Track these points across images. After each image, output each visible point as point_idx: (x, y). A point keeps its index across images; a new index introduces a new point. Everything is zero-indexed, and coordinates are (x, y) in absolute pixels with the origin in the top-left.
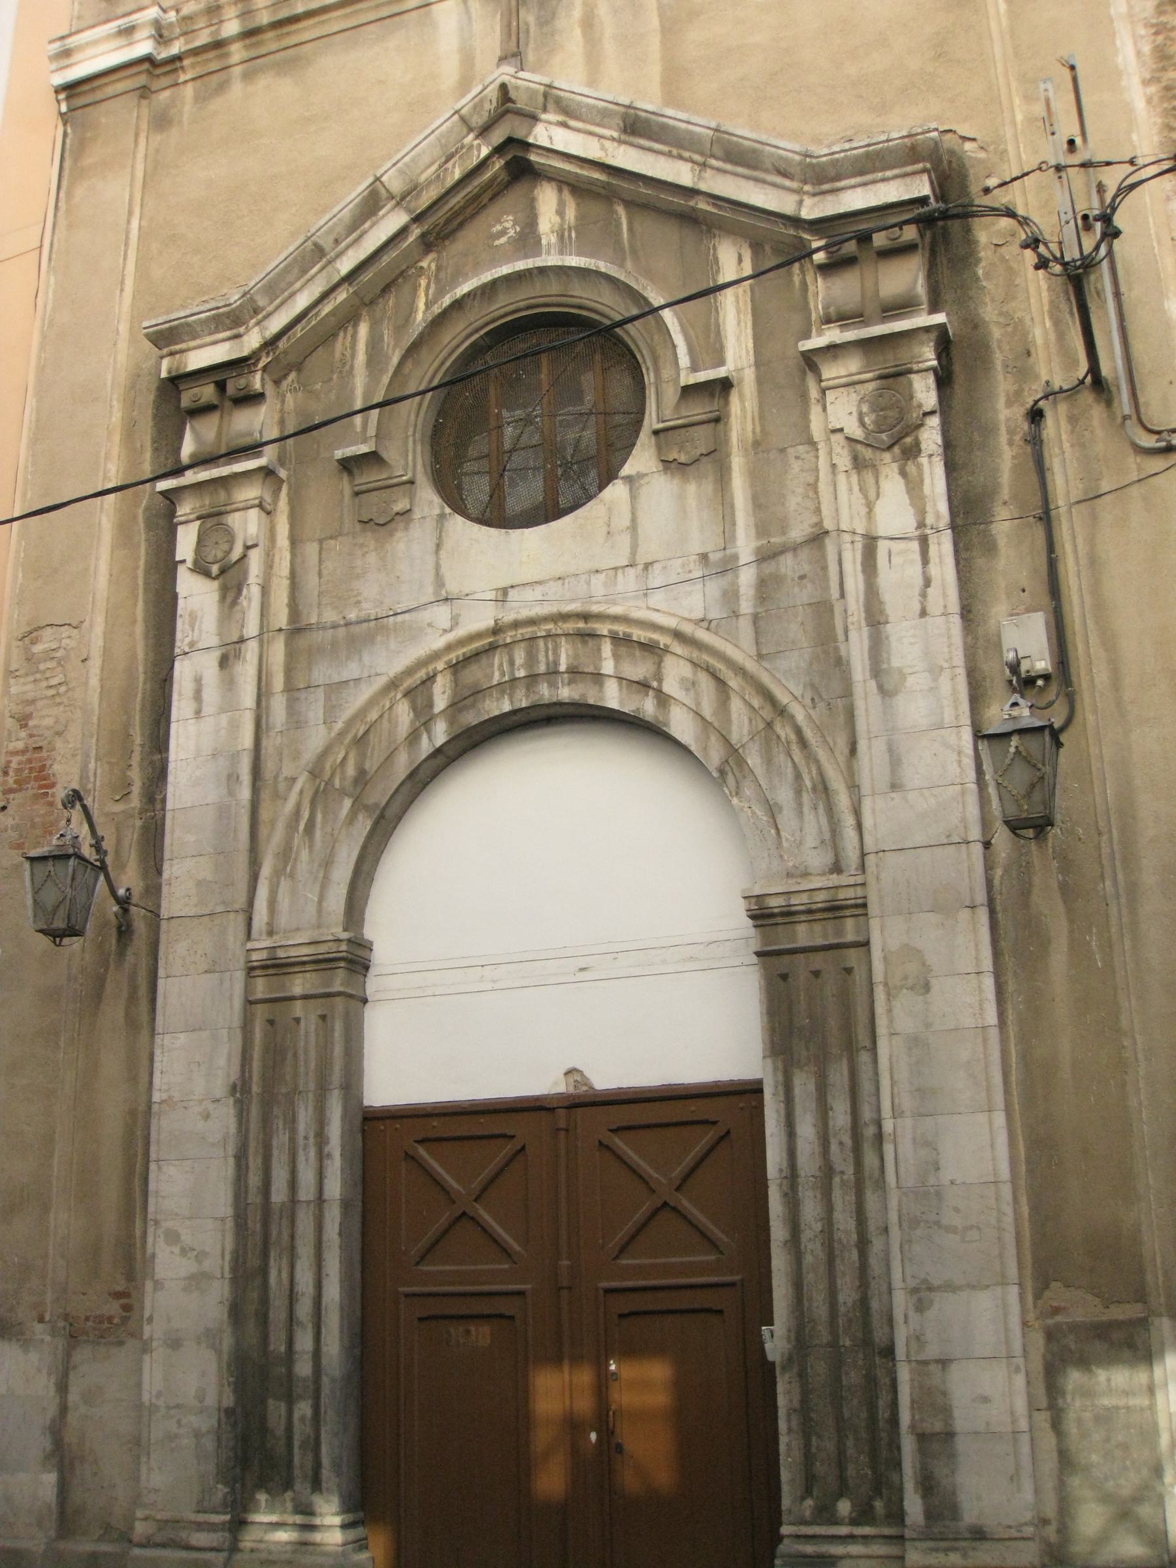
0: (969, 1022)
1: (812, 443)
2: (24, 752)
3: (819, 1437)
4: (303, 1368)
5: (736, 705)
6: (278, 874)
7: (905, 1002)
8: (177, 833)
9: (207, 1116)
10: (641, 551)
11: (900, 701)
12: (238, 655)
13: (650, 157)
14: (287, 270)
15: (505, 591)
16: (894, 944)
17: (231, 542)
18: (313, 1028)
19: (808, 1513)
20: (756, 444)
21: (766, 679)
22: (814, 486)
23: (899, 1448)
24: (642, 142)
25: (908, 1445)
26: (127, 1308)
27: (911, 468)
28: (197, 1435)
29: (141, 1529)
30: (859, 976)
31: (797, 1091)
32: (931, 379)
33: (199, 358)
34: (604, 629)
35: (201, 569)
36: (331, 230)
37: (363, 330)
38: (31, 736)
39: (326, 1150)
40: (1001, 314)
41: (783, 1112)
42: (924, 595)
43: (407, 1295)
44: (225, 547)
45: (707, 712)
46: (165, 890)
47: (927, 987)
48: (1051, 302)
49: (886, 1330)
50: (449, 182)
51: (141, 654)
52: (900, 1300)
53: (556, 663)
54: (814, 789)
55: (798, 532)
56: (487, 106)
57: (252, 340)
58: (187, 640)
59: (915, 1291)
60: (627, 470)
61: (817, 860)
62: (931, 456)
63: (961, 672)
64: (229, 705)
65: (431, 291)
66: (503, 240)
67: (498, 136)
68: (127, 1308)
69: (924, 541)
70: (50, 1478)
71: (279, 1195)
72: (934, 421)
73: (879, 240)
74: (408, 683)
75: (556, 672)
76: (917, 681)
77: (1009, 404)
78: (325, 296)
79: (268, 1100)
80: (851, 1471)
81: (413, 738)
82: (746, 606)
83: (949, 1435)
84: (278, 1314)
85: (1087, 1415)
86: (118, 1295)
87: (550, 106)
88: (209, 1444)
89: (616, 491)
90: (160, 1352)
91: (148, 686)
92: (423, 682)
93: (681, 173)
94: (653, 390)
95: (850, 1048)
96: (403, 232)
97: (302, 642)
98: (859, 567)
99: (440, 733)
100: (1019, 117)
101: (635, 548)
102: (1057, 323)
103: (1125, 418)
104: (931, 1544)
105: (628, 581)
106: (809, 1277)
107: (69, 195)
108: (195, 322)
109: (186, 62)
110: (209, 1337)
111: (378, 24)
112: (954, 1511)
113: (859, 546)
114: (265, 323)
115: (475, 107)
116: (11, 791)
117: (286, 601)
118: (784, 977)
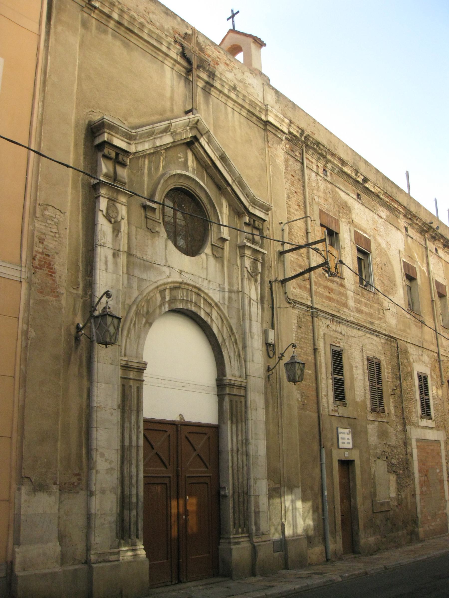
1: (238, 267)
4: (134, 500)
14: (146, 133)
28: (110, 523)
34: (202, 295)
38: (45, 248)
45: (220, 327)
58: (102, 241)
59: (255, 479)
65: (164, 162)
68: (80, 480)
71: (127, 443)
72: (259, 275)
74: (160, 288)
75: (192, 302)
76: (256, 337)
86: (77, 475)
88: (114, 526)
90: (98, 495)
91: (84, 249)
105: (206, 282)
108: (121, 129)
109: (96, 11)
111: (151, 56)
117: (127, 242)
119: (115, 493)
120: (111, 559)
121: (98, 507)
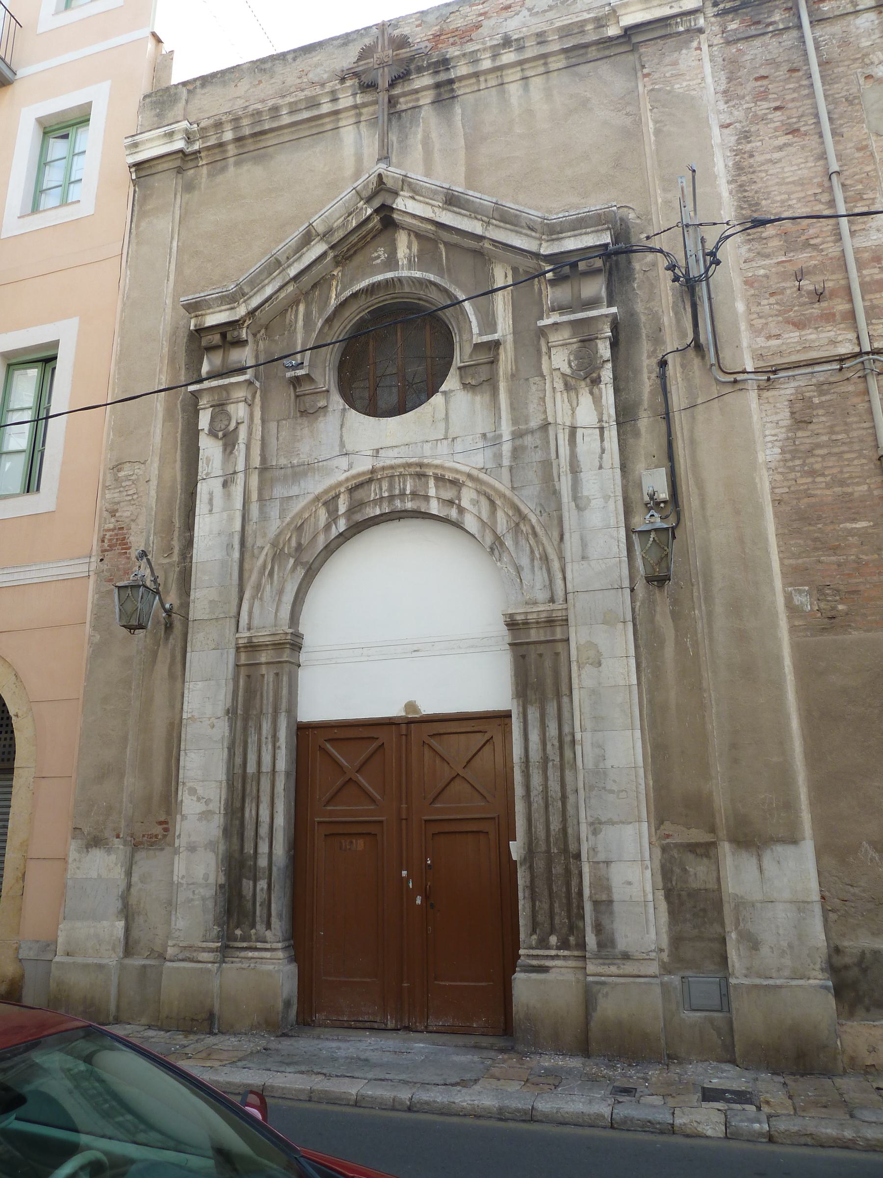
0: (622, 683)
1: (543, 376)
2: (113, 530)
3: (541, 901)
4: (263, 862)
5: (500, 514)
6: (253, 598)
7: (588, 670)
8: (199, 575)
9: (213, 727)
10: (450, 431)
11: (587, 513)
12: (233, 481)
13: (459, 218)
14: (260, 272)
15: (377, 451)
16: (582, 641)
17: (230, 420)
18: (271, 679)
19: (534, 943)
20: (513, 375)
21: (516, 500)
22: (543, 399)
23: (583, 908)
24: (455, 209)
25: (588, 907)
26: (166, 830)
27: (596, 390)
28: (204, 899)
29: (170, 951)
30: (563, 658)
31: (530, 717)
32: (608, 343)
33: (211, 320)
34: (430, 472)
35: (213, 433)
36: (285, 252)
37: (302, 308)
38: (117, 521)
39: (278, 744)
40: (646, 309)
41: (522, 727)
42: (601, 458)
43: (319, 823)
44: (226, 423)
46: (191, 605)
47: (600, 664)
48: (674, 302)
49: (576, 844)
50: (350, 228)
51: (179, 478)
52: (584, 829)
53: (405, 489)
54: (541, 559)
55: (534, 423)
56: (371, 186)
57: (241, 311)
58: (205, 472)
59: (592, 824)
60: (443, 388)
61: (542, 595)
62: (606, 384)
63: (620, 499)
64: (228, 507)
66: (379, 261)
67: (377, 203)
68: (166, 830)
69: (602, 429)
70: (121, 924)
71: (251, 768)
72: (609, 365)
73: (582, 266)
74: (325, 498)
75: (405, 494)
76: (597, 503)
77: (649, 357)
78: (281, 288)
79: (246, 719)
80: (557, 920)
81: (327, 527)
82: (506, 462)
83: (610, 902)
84: (249, 833)
85: (684, 893)
86: (161, 823)
87: (405, 187)
88: (210, 904)
89: (437, 399)
90: (184, 854)
92: (333, 498)
93: (476, 227)
94: (458, 345)
95: (558, 695)
96: (324, 255)
97: (268, 475)
98: (567, 442)
99: (342, 525)
100: (660, 200)
101: (447, 429)
102: (676, 314)
103: (712, 365)
104: (601, 961)
105: (443, 448)
106: (535, 816)
107: (137, 226)
109: (202, 154)
110: (211, 845)
112: (612, 943)
113: (567, 431)
114: (249, 302)
115: (364, 186)
116: (106, 551)
117: (259, 453)
118: (523, 657)
119: (214, 852)
120: (200, 959)
121: (183, 872)
